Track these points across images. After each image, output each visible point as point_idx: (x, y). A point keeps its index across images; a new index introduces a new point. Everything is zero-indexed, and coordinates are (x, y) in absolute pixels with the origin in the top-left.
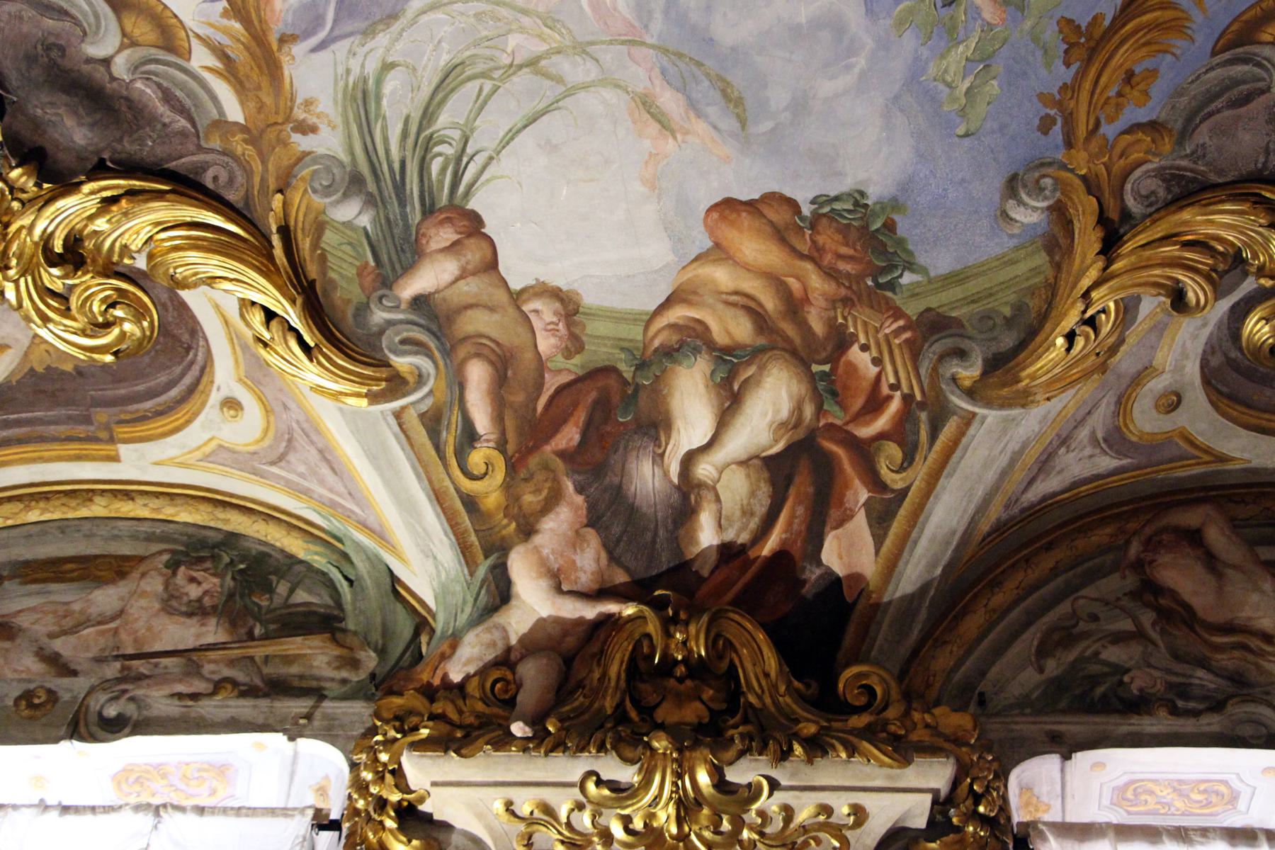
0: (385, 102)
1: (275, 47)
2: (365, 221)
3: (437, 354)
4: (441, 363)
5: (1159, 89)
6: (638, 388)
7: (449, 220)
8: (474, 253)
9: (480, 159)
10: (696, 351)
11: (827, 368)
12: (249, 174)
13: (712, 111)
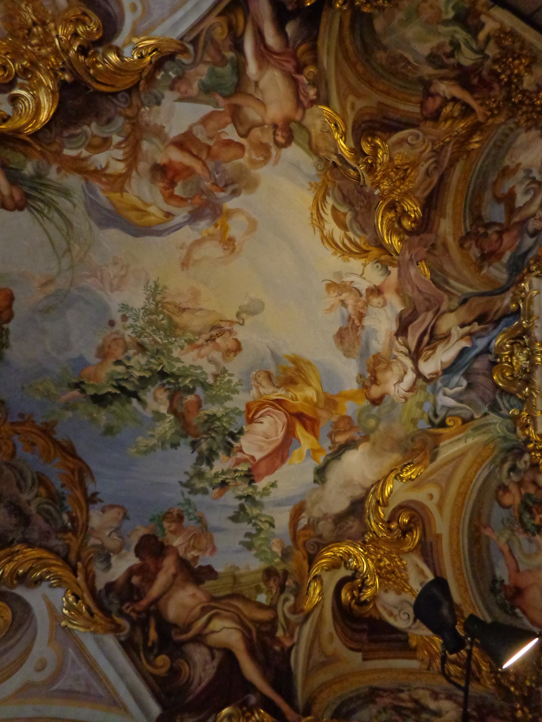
0: (63, 199)
1: (85, 176)
9: (41, 220)
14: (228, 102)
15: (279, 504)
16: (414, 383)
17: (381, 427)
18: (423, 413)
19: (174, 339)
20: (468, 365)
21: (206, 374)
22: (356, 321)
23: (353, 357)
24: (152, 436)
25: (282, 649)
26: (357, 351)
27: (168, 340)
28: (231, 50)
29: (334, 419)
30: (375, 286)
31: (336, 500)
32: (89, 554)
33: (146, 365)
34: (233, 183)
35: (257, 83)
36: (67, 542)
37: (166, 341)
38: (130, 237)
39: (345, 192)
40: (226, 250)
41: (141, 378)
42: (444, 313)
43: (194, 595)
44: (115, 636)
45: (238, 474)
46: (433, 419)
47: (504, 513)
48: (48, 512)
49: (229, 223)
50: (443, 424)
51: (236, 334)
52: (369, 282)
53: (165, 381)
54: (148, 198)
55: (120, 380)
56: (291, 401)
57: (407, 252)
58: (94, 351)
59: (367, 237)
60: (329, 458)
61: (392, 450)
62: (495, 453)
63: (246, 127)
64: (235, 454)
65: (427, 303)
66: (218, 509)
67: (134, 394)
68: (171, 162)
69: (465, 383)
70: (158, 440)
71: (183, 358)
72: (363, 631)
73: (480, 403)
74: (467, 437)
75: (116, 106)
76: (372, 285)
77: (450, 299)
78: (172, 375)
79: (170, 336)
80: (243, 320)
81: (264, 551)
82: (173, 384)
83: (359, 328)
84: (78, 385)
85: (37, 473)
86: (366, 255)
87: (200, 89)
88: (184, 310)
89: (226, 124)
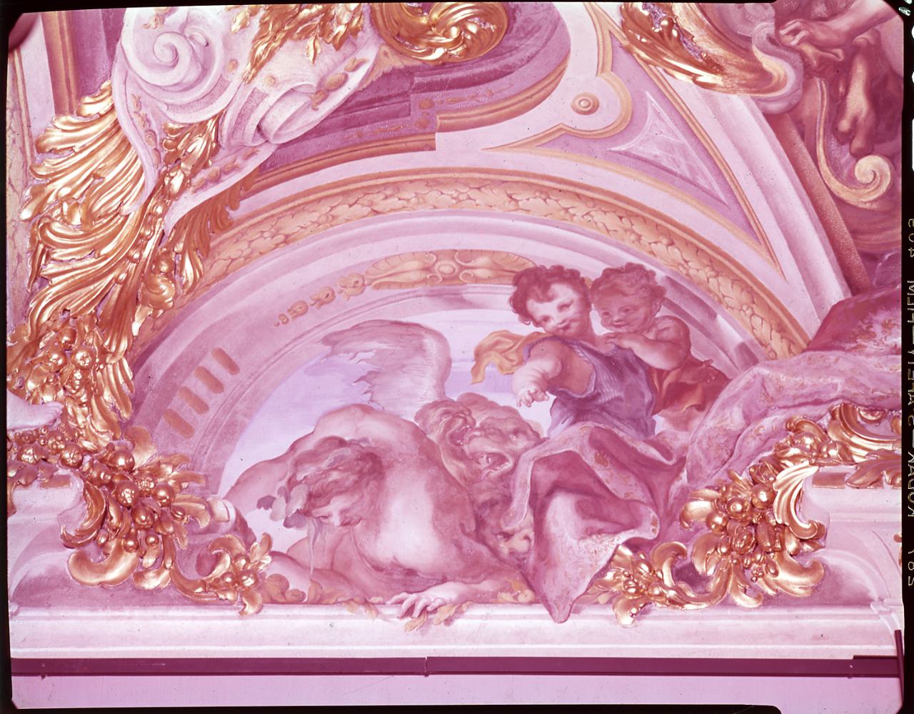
44: (758, 101)
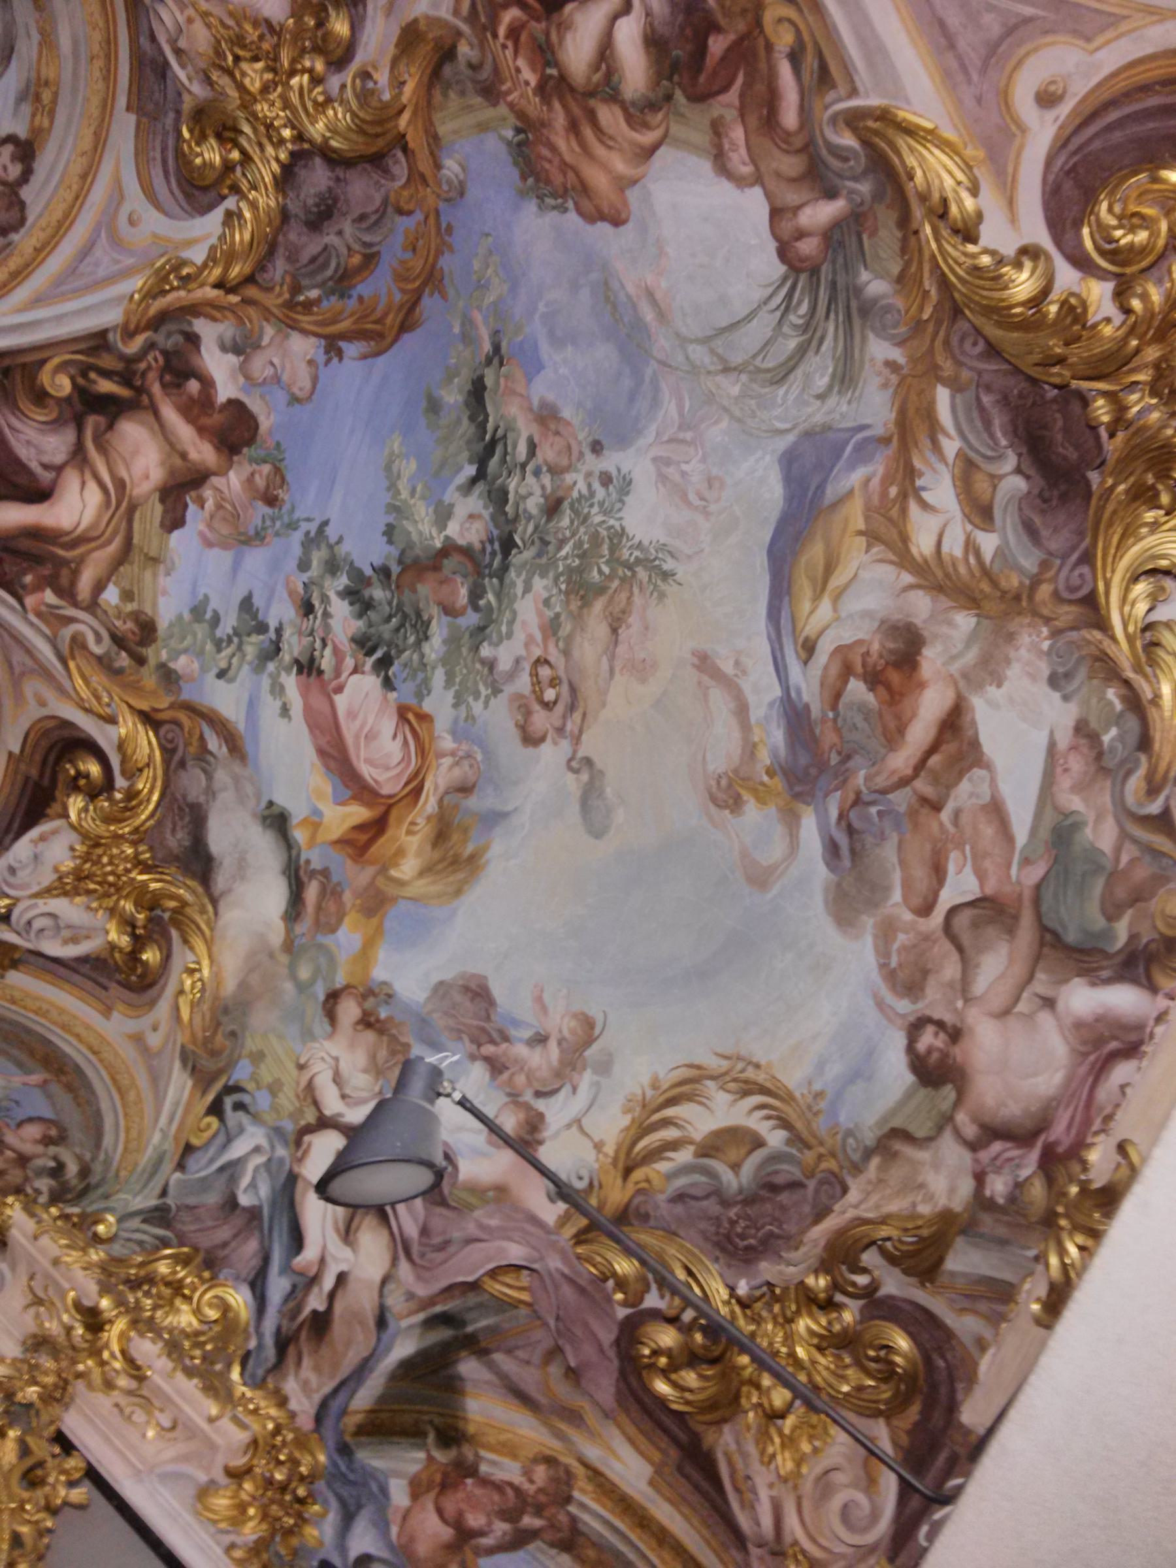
0: (830, 370)
2: (865, 276)
3: (821, 143)
4: (818, 132)
5: (398, 240)
6: (670, 79)
7: (802, 260)
8: (786, 227)
10: (633, 104)
11: (549, 71)
12: (947, 343)
13: (622, 297)
14: (1027, 894)
15: (252, 705)
16: (316, 1103)
17: (289, 986)
18: (258, 1083)
19: (563, 587)
20: (266, 1232)
21: (497, 645)
22: (488, 1049)
23: (428, 999)
24: (413, 493)
25: (24, 587)
26: (435, 1016)
27: (562, 574)
28: (1133, 937)
29: (347, 896)
30: (540, 1143)
31: (232, 832)
32: (250, 321)
33: (525, 511)
34: (853, 851)
35: (1049, 1003)
36: (277, 289)
37: (561, 569)
38: (767, 536)
39: (784, 1198)
40: (718, 783)
41: (504, 493)
42: (394, 1261)
43: (147, 477)
45: (318, 644)
46: (236, 1097)
47: (20, 1114)
48: (325, 265)
49: (772, 810)
50: (216, 1109)
51: (555, 743)
52: (557, 1134)
53: (497, 546)
54: (853, 604)
55: (505, 445)
56: (409, 819)
57: (566, 1271)
58: (551, 397)
59: (661, 1198)
60: (294, 853)
61: (243, 985)
62: (111, 1174)
63: (966, 939)
64: (354, 656)
65: (437, 1240)
66: (268, 577)
67: (480, 475)
68: (922, 685)
69: (244, 1200)
70: (405, 501)
71: (529, 596)
72: (41, 775)
73: (191, 1201)
74: (165, 1135)
75: (1064, 557)
76: (546, 1134)
77: (410, 1296)
78: (505, 568)
79: (568, 582)
80: (576, 771)
81: (183, 638)
82: (490, 565)
83: (474, 1047)
84: (497, 348)
85: (378, 253)
86: (621, 1165)
87: (1067, 816)
88: (615, 631)
89: (981, 875)
